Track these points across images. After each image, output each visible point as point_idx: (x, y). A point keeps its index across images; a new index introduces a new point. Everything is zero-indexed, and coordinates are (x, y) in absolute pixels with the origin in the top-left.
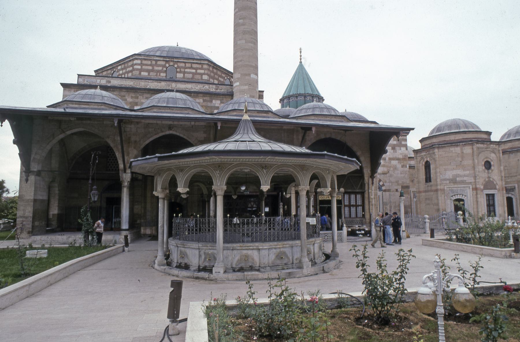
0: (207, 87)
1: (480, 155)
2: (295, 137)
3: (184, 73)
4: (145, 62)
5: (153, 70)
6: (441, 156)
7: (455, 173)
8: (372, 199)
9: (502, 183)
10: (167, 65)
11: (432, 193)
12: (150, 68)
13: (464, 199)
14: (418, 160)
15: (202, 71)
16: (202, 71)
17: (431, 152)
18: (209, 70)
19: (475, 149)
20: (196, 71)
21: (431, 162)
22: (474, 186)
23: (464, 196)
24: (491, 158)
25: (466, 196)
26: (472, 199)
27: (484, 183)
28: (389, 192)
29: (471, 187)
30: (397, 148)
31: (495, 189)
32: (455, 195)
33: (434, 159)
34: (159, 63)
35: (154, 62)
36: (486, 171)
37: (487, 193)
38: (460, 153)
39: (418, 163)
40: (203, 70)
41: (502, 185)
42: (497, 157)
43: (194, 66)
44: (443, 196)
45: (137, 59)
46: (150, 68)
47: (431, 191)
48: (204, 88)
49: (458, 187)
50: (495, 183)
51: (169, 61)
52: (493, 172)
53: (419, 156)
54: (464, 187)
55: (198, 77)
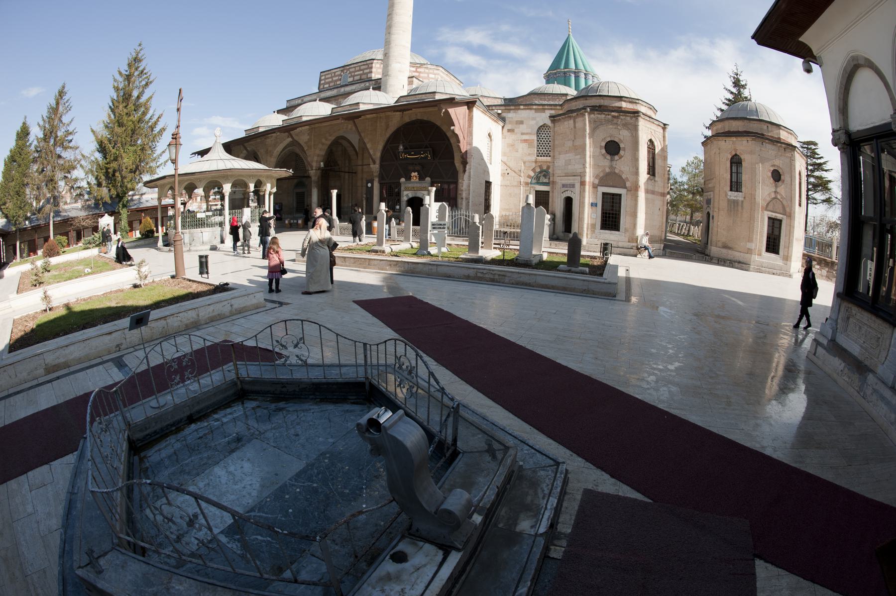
2: (378, 125)
3: (354, 76)
4: (327, 77)
5: (331, 82)
8: (462, 190)
12: (330, 80)
27: (601, 175)
31: (625, 188)
35: (333, 75)
36: (608, 157)
46: (330, 80)
50: (624, 177)
55: (364, 77)
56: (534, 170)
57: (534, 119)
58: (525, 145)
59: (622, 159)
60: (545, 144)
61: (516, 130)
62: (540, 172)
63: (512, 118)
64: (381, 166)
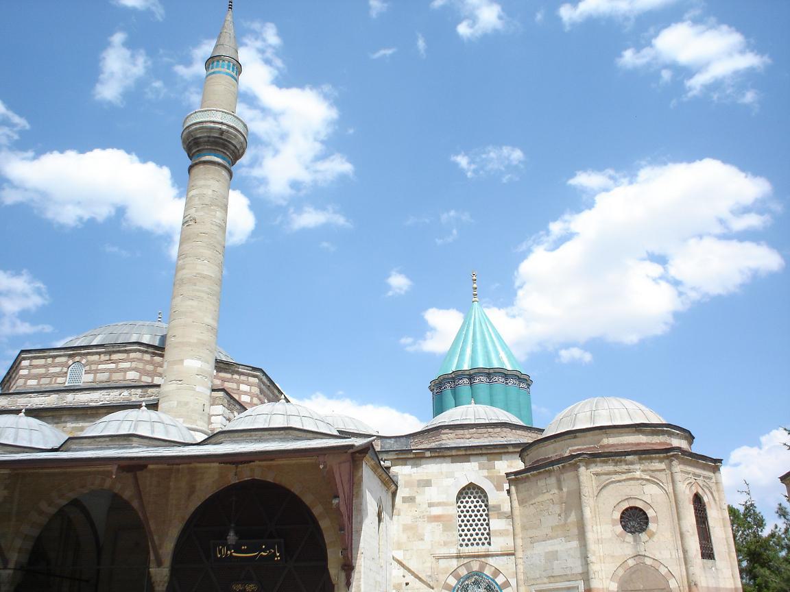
0: (126, 393)
1: (604, 492)
3: (96, 372)
4: (35, 362)
7: (550, 549)
10: (70, 362)
12: (42, 371)
15: (126, 365)
16: (127, 365)
18: (140, 360)
20: (117, 366)
27: (621, 572)
34: (58, 360)
36: (629, 537)
40: (129, 361)
43: (115, 357)
45: (24, 359)
46: (42, 371)
48: (121, 396)
50: (663, 571)
51: (73, 354)
55: (117, 376)
56: (454, 573)
57: (450, 475)
58: (437, 527)
59: (655, 539)
60: (474, 520)
61: (418, 499)
62: (468, 578)
63: (411, 475)
64: (174, 571)
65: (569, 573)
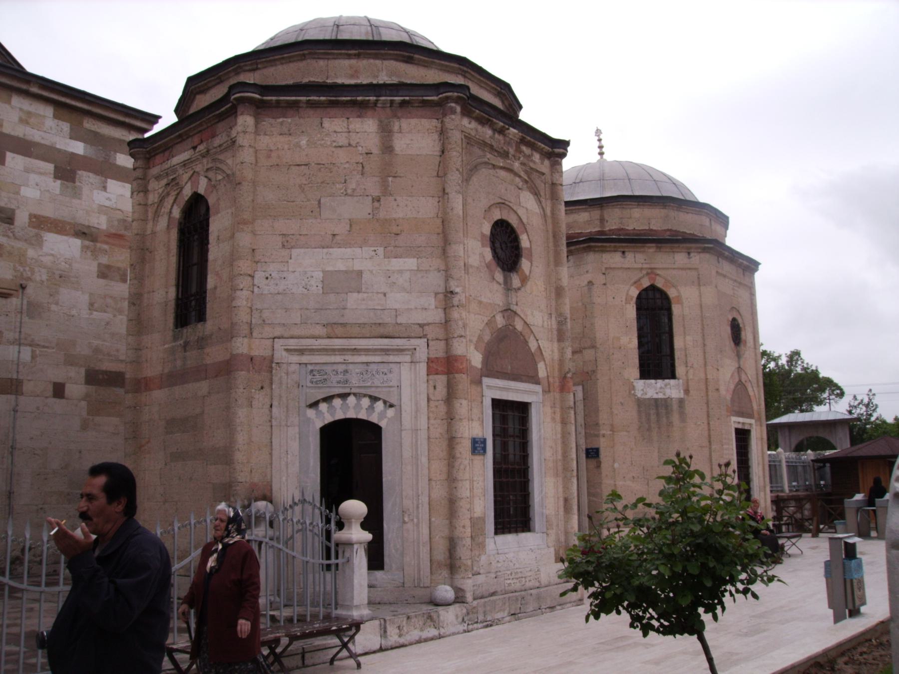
1: (475, 179)
6: (269, 157)
7: (341, 266)
9: (562, 351)
11: (203, 387)
13: (383, 424)
14: (153, 198)
17: (217, 141)
19: (456, 137)
21: (211, 201)
22: (438, 350)
23: (379, 405)
24: (521, 212)
25: (391, 406)
26: (423, 422)
28: (12, 397)
29: (422, 354)
30: (86, 178)
31: (534, 379)
32: (328, 399)
33: (232, 180)
37: (499, 395)
38: (375, 151)
39: (150, 215)
41: (561, 362)
42: (545, 215)
44: (260, 398)
47: (200, 372)
49: (355, 351)
50: (533, 345)
52: (529, 284)
53: (158, 178)
54: (386, 351)
65: (388, 320)
